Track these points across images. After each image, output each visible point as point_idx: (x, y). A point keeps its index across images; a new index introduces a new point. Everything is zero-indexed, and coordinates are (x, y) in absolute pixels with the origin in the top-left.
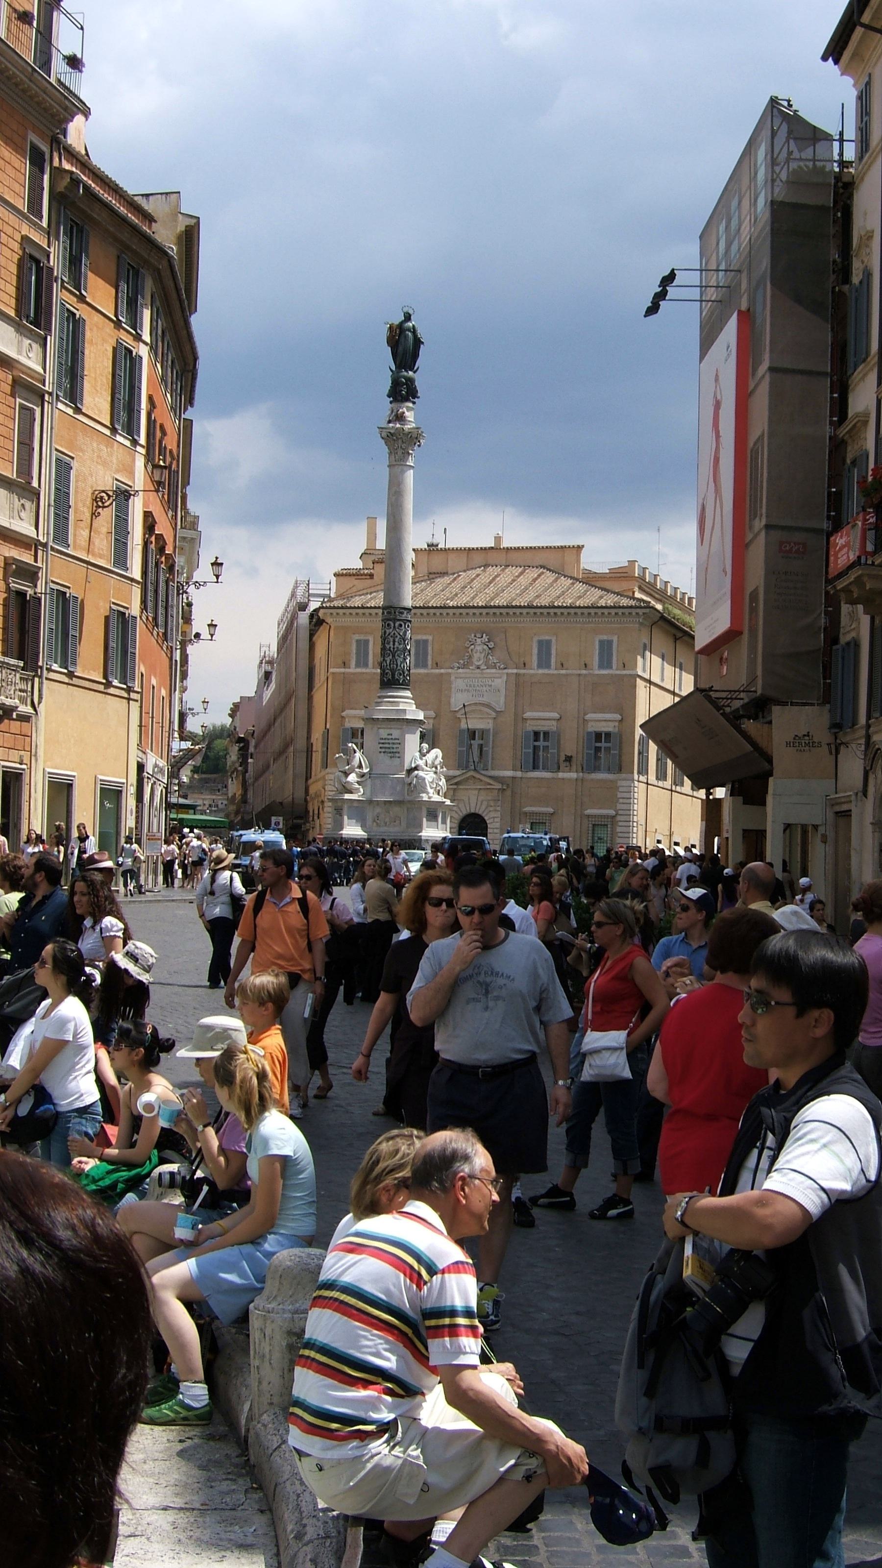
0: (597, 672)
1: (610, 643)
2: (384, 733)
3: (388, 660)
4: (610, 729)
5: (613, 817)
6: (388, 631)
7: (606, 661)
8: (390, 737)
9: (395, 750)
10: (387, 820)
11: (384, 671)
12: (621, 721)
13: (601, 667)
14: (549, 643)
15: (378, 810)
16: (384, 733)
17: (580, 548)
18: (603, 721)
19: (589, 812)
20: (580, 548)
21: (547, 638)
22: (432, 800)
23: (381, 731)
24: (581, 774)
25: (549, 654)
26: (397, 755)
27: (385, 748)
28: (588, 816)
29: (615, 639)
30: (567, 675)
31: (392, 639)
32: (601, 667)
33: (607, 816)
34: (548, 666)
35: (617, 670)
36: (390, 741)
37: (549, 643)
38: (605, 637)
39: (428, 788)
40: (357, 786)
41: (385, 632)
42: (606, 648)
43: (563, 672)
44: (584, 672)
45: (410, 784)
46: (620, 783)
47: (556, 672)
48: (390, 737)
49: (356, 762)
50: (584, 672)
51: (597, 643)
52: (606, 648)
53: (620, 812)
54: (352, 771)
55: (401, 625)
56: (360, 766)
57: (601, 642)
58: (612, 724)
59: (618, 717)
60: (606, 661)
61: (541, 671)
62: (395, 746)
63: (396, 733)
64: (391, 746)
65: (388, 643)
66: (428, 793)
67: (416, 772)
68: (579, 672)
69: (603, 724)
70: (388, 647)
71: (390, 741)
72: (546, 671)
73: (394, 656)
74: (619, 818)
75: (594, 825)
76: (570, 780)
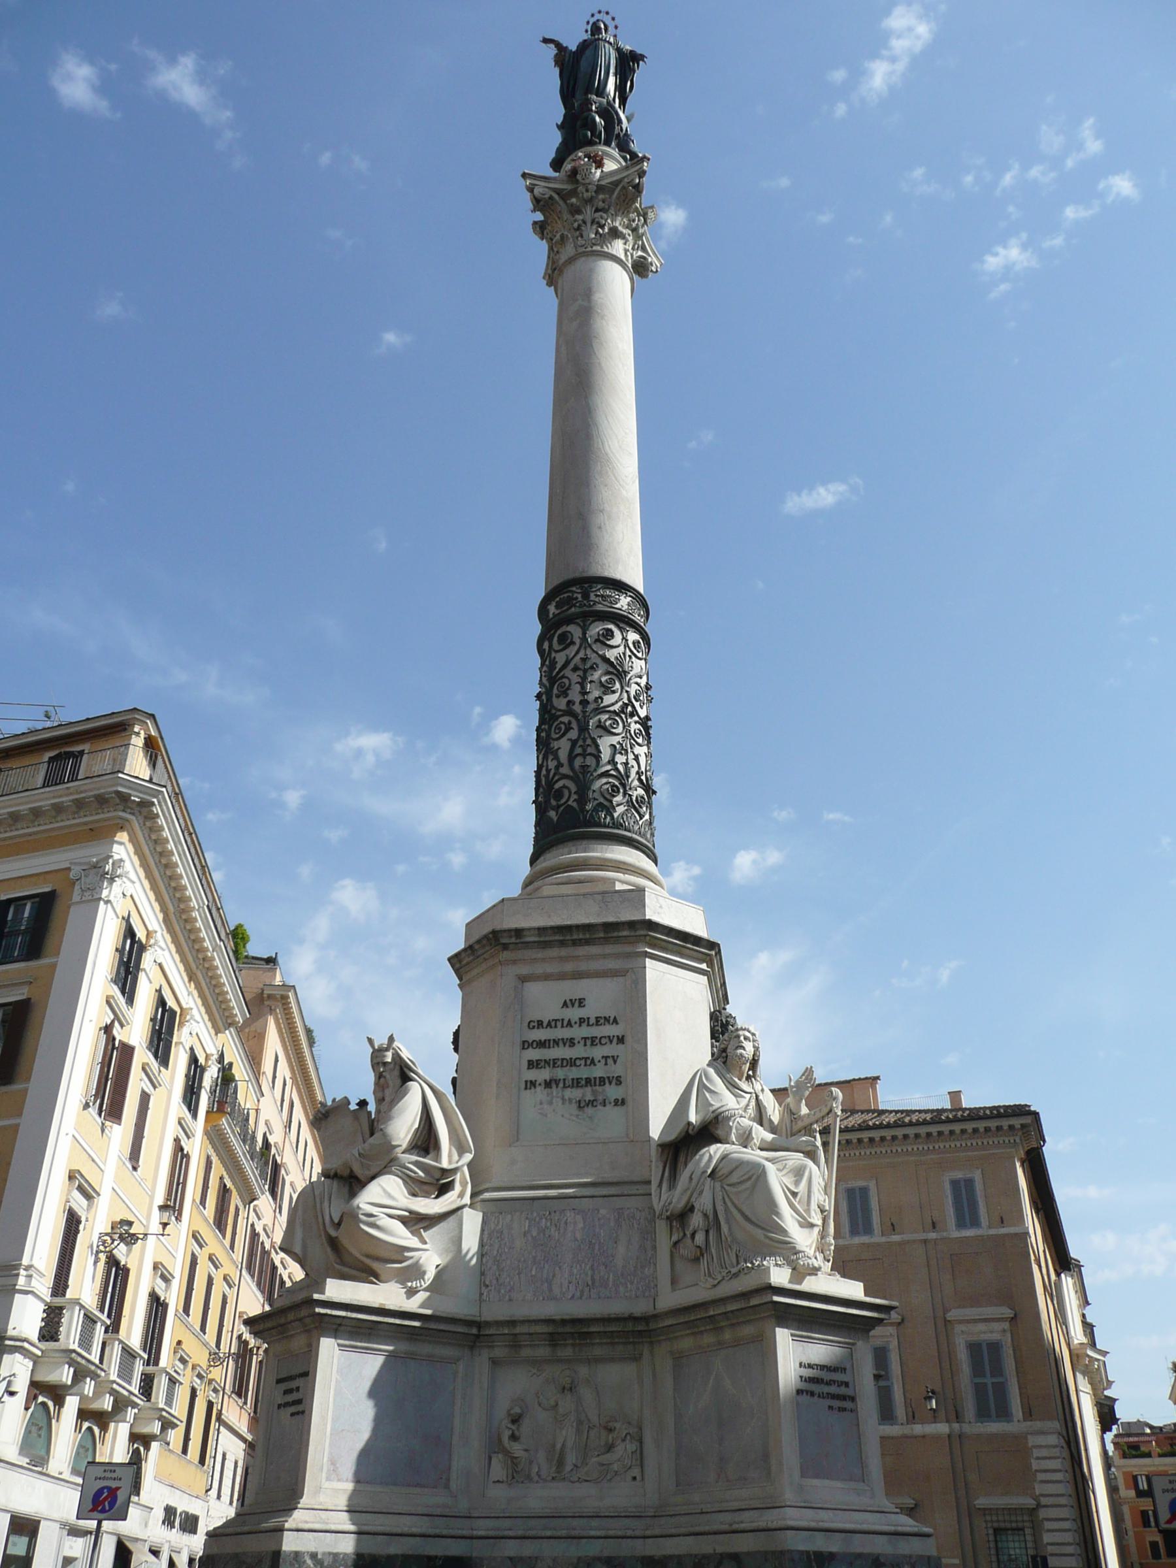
0: (956, 1234)
1: (969, 1183)
2: (545, 1000)
3: (563, 746)
4: (995, 1337)
5: (1033, 1511)
6: (560, 658)
7: (967, 1214)
8: (574, 1014)
9: (598, 1072)
10: (567, 1435)
11: (550, 784)
12: (1013, 1320)
13: (961, 1224)
14: (864, 1191)
15: (517, 1384)
16: (545, 1000)
17: (878, 1078)
18: (981, 1324)
19: (981, 1502)
20: (878, 1078)
21: (861, 1183)
22: (810, 1285)
23: (534, 990)
24: (956, 1426)
25: (866, 1211)
26: (612, 1092)
27: (553, 1063)
28: (985, 1511)
29: (977, 1176)
30: (902, 1244)
31: (575, 678)
32: (961, 1224)
33: (1020, 1510)
34: (868, 1230)
35: (990, 1227)
36: (578, 1032)
37: (864, 1191)
38: (959, 1175)
39: (789, 1220)
40: (401, 1235)
41: (553, 663)
42: (964, 1193)
43: (896, 1238)
44: (933, 1235)
45: (682, 1217)
46: (1032, 1441)
47: (884, 1239)
48: (574, 1014)
49: (403, 1126)
50: (933, 1235)
51: (947, 1186)
52: (964, 1193)
53: (1044, 1501)
54: (382, 1161)
55: (609, 634)
56: (426, 1141)
57: (955, 1183)
58: (996, 1326)
59: (1007, 1312)
60: (967, 1214)
61: (857, 1240)
62: (598, 1052)
63: (599, 996)
64: (579, 1051)
65: (564, 693)
66: (788, 1252)
67: (715, 1151)
68: (923, 1236)
69: (981, 1327)
70: (561, 703)
71: (578, 1032)
72: (865, 1239)
73: (584, 728)
74: (1042, 1514)
75: (996, 1531)
76: (936, 1438)
